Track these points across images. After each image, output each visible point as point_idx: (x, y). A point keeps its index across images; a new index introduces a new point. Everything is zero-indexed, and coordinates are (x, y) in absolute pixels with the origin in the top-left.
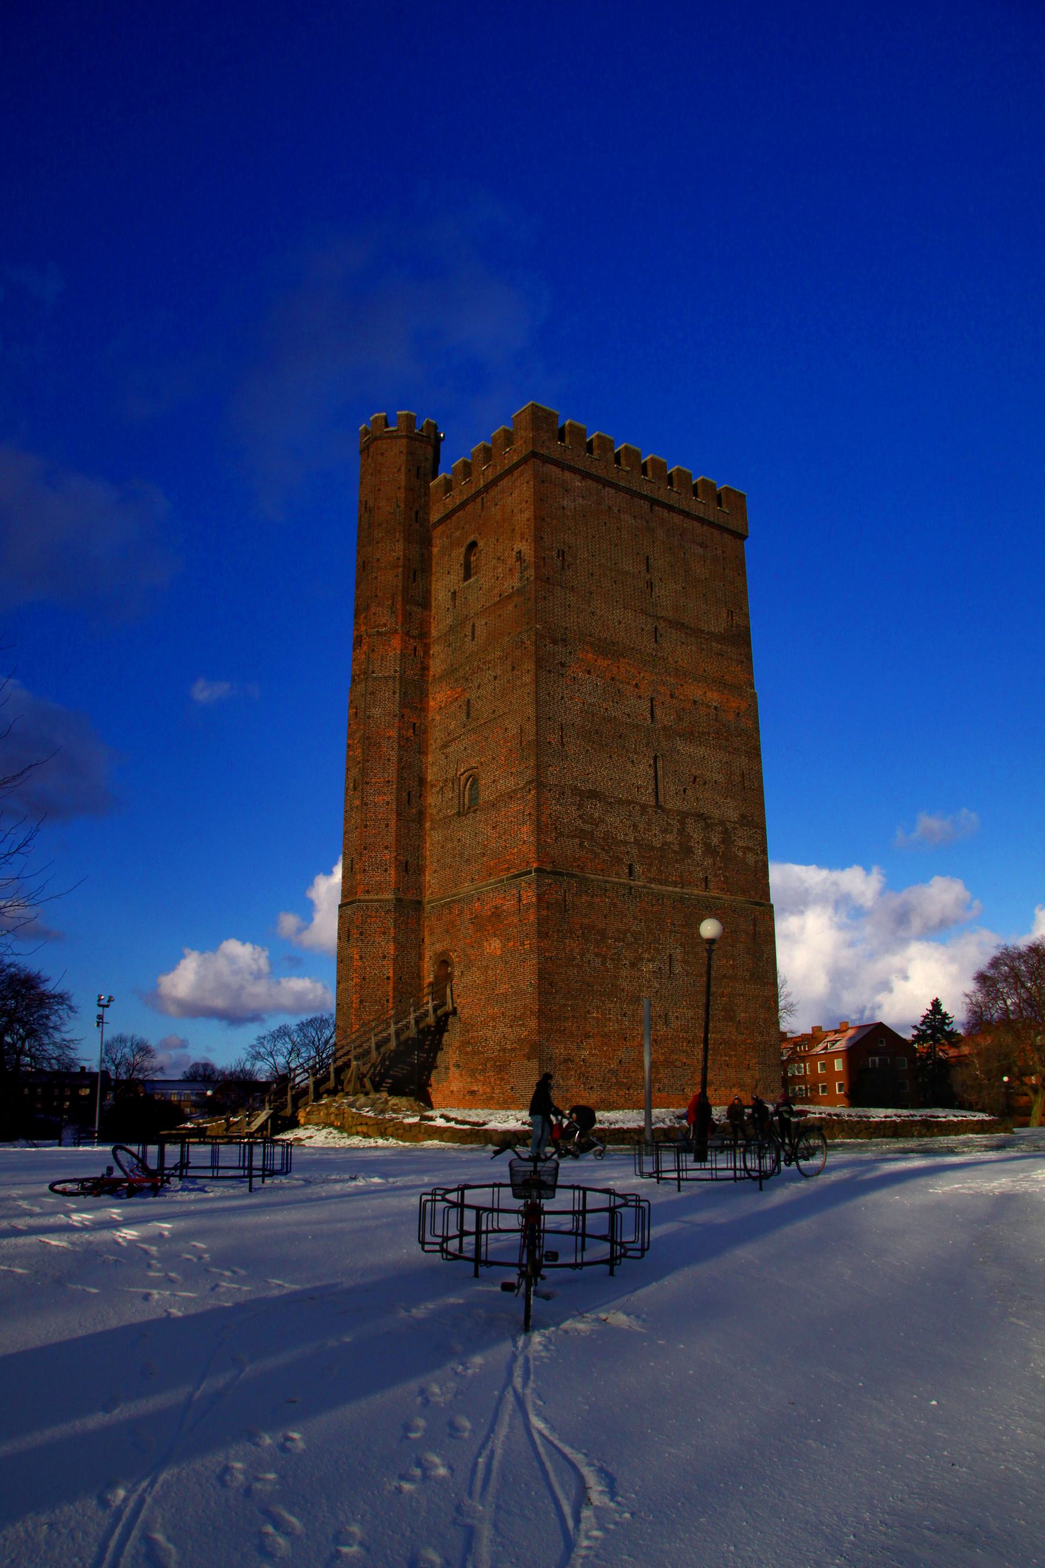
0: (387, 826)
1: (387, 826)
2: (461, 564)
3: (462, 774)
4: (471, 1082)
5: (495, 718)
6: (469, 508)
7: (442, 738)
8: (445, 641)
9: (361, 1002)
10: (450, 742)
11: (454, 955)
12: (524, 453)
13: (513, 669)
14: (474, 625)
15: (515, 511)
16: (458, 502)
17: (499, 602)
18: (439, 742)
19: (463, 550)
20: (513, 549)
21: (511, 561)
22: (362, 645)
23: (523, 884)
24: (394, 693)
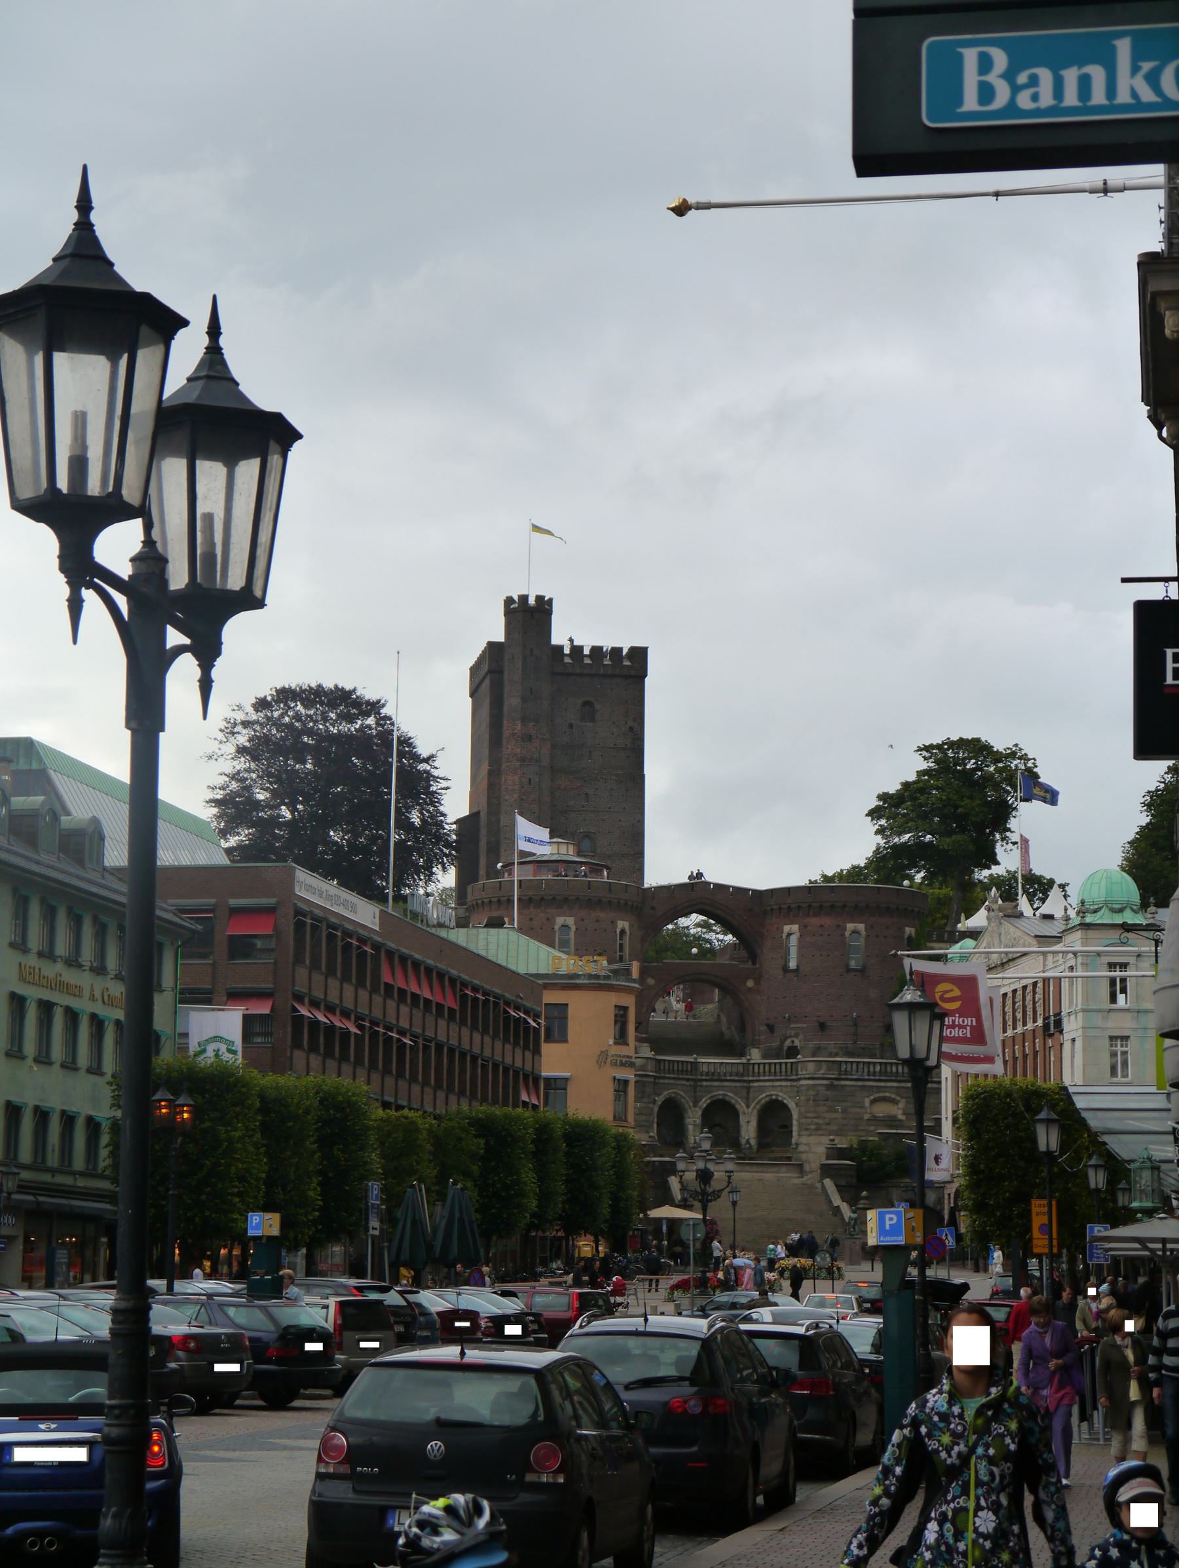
13: (627, 790)
16: (578, 671)
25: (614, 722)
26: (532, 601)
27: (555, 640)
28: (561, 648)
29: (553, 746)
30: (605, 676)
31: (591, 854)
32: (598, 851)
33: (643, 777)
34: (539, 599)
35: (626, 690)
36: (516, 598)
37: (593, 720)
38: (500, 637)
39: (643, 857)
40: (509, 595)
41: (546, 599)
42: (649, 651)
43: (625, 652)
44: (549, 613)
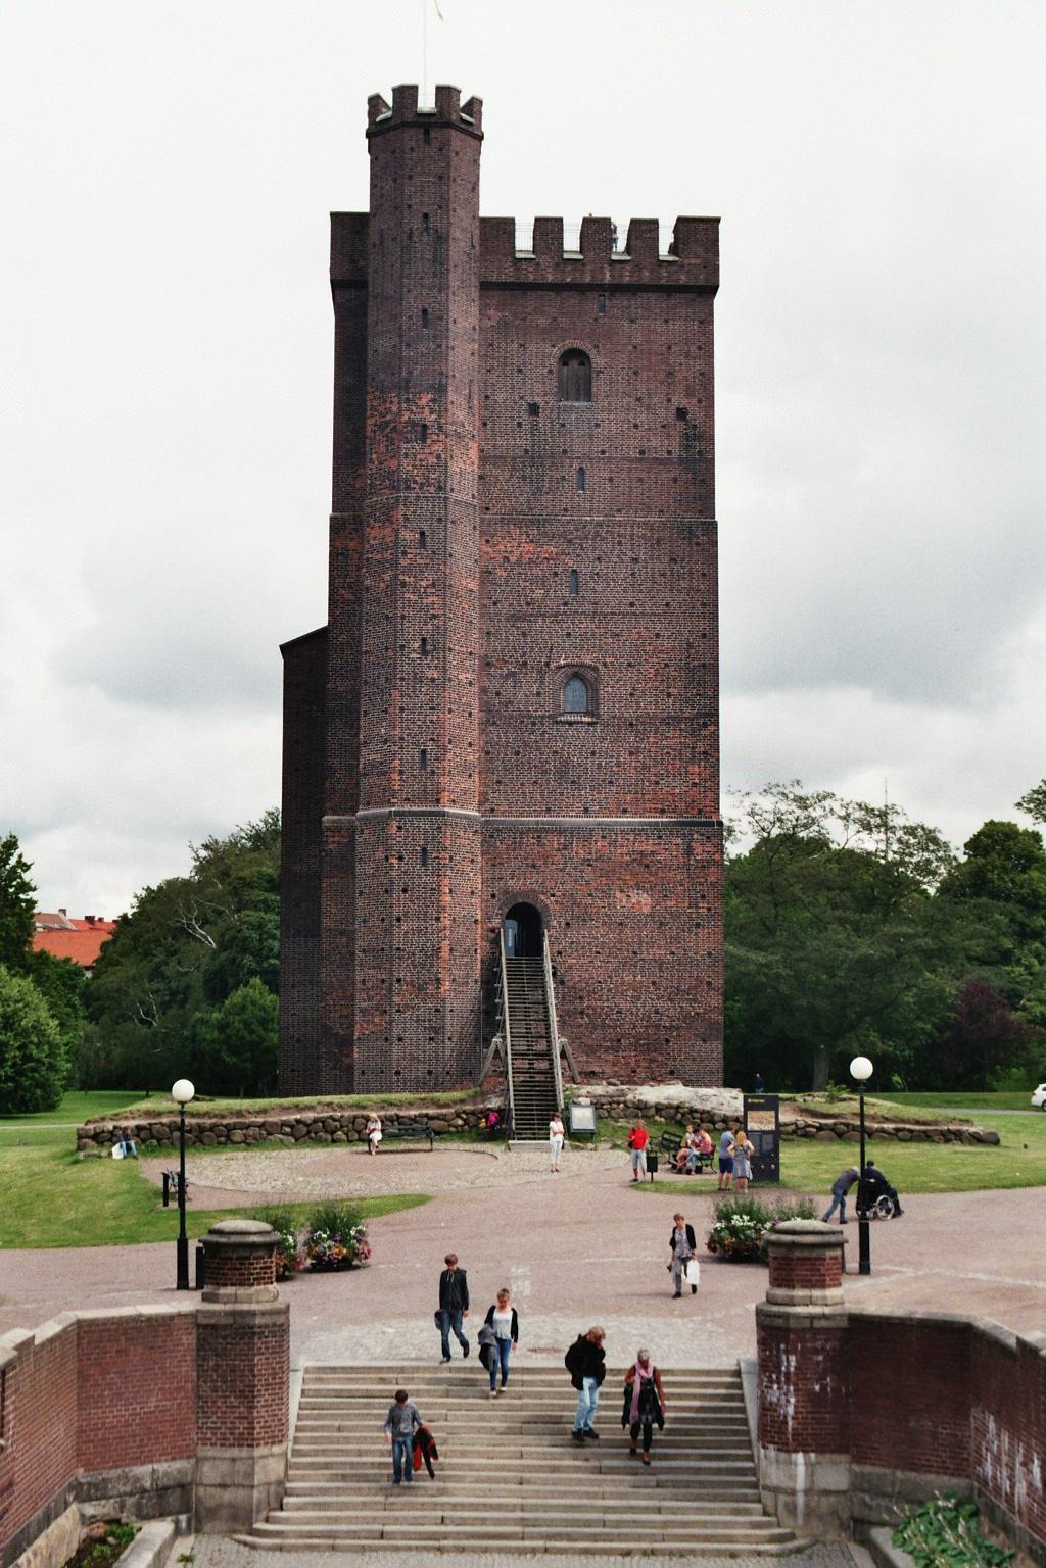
0: (470, 714)
1: (470, 714)
2: (550, 371)
3: (559, 667)
4: (587, 1061)
5: (635, 614)
7: (511, 605)
9: (451, 950)
10: (532, 615)
12: (701, 280)
13: (673, 560)
14: (581, 470)
15: (674, 349)
16: (550, 278)
17: (641, 460)
18: (503, 608)
19: (556, 352)
20: (669, 400)
21: (667, 415)
22: (429, 441)
23: (695, 836)
24: (475, 527)
25: (639, 400)
26: (426, 102)
27: (489, 208)
29: (484, 458)
30: (616, 289)
31: (587, 719)
32: (603, 709)
33: (711, 528)
34: (445, 93)
35: (666, 321)
36: (389, 99)
38: (361, 204)
40: (373, 93)
42: (723, 229)
43: (666, 239)
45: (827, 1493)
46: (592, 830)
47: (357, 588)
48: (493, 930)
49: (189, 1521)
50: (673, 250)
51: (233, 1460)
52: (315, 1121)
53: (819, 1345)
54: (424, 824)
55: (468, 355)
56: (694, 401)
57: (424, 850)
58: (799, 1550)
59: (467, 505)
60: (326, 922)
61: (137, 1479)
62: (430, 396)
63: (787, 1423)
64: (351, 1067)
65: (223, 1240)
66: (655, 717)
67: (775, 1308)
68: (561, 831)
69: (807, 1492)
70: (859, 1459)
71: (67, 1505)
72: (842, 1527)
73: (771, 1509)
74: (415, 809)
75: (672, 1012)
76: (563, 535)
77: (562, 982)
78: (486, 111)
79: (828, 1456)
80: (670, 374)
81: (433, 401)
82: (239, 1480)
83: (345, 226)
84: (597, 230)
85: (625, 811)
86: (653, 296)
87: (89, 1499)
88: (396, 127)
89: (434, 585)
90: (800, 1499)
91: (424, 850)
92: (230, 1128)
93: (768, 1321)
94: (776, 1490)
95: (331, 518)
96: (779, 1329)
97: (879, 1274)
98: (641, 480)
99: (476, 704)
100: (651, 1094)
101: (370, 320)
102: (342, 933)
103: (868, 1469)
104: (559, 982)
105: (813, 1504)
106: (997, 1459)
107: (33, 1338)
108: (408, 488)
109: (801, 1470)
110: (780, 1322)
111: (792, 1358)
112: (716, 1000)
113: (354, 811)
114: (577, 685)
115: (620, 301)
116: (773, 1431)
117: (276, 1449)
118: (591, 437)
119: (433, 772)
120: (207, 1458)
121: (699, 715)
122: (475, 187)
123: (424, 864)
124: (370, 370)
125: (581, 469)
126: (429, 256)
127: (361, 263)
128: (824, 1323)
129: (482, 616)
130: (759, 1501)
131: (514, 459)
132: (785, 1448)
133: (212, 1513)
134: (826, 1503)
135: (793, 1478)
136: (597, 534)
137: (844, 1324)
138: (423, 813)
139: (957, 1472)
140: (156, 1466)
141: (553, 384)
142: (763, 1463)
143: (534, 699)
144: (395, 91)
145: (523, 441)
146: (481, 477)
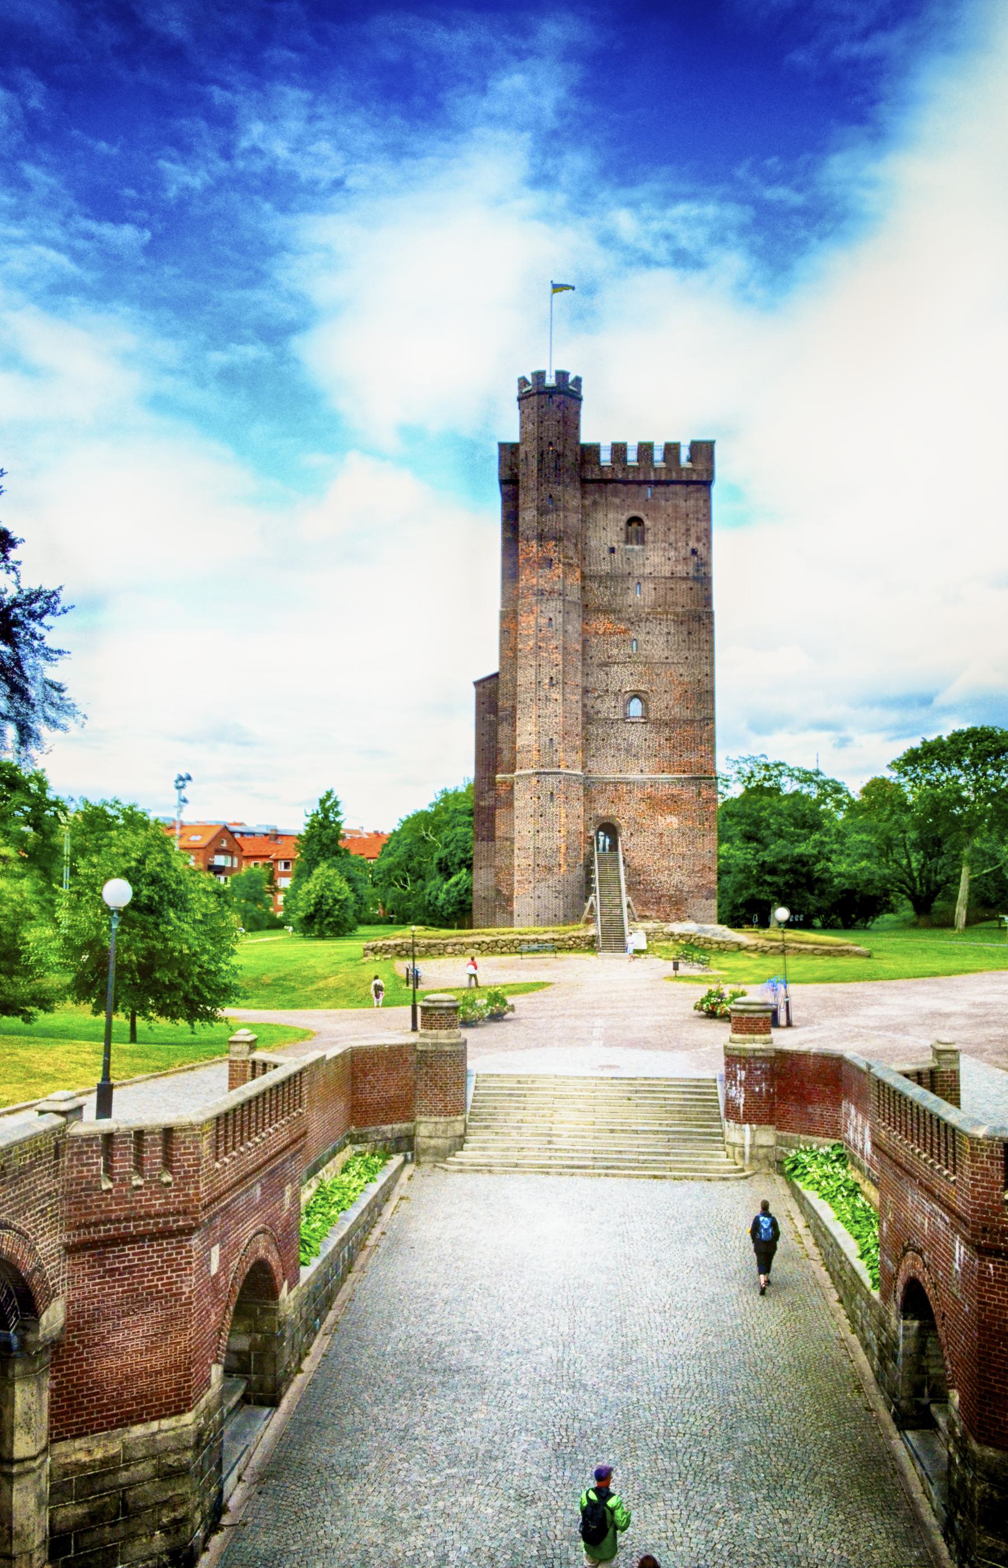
3: (626, 692)
6: (634, 488)
8: (601, 582)
11: (622, 822)
12: (704, 478)
13: (689, 633)
15: (691, 516)
16: (620, 476)
17: (671, 578)
19: (625, 518)
20: (687, 544)
21: (686, 552)
25: (670, 544)
28: (593, 450)
30: (657, 483)
31: (643, 720)
32: (652, 715)
33: (710, 615)
34: (562, 376)
36: (530, 379)
37: (642, 541)
39: (714, 723)
40: (520, 375)
41: (571, 378)
43: (684, 454)
44: (576, 397)
45: (762, 1147)
46: (645, 783)
47: (515, 650)
48: (590, 837)
49: (413, 1155)
50: (690, 460)
51: (436, 1123)
52: (492, 941)
53: (758, 1065)
54: (550, 779)
55: (575, 521)
56: (701, 544)
57: (552, 793)
58: (746, 1177)
59: (575, 603)
60: (498, 833)
61: (384, 1133)
62: (554, 543)
63: (739, 1108)
64: (512, 913)
65: (431, 1005)
66: (680, 720)
67: (734, 1045)
68: (628, 783)
69: (752, 1146)
70: (780, 1128)
71: (345, 1146)
72: (771, 1165)
73: (731, 1155)
74: (547, 770)
75: (690, 883)
76: (629, 620)
77: (629, 866)
78: (583, 384)
79: (763, 1126)
80: (688, 530)
81: (556, 546)
82: (439, 1133)
83: (509, 452)
84: (645, 450)
85: (663, 771)
86: (678, 488)
87: (357, 1143)
88: (533, 395)
89: (557, 648)
90: (747, 1150)
91: (552, 793)
92: (446, 945)
93: (730, 1052)
94: (734, 1145)
95: (502, 612)
96: (737, 1057)
97: (795, 1027)
98: (672, 589)
99: (580, 712)
100: (676, 928)
101: (521, 501)
102: (507, 839)
103: (785, 1134)
104: (627, 866)
105: (754, 1152)
106: (856, 1130)
107: (325, 1056)
108: (543, 594)
109: (748, 1134)
110: (736, 1053)
111: (743, 1073)
112: (714, 877)
113: (513, 771)
114: (636, 701)
115: (661, 489)
116: (731, 1112)
117: (459, 1118)
118: (644, 565)
119: (556, 751)
120: (421, 1122)
121: (704, 719)
122: (577, 427)
123: (552, 800)
124: (521, 529)
125: (639, 583)
126: (552, 465)
127: (516, 470)
128: (760, 1054)
129: (583, 665)
130: (725, 1150)
131: (601, 577)
132: (738, 1121)
133: (425, 1151)
134: (762, 1152)
135: (743, 1138)
136: (647, 619)
137: (773, 1054)
138: (551, 773)
139: (835, 1136)
140: (395, 1126)
141: (623, 536)
142: (727, 1130)
143: (613, 710)
144: (533, 374)
145: (605, 568)
146: (583, 588)
